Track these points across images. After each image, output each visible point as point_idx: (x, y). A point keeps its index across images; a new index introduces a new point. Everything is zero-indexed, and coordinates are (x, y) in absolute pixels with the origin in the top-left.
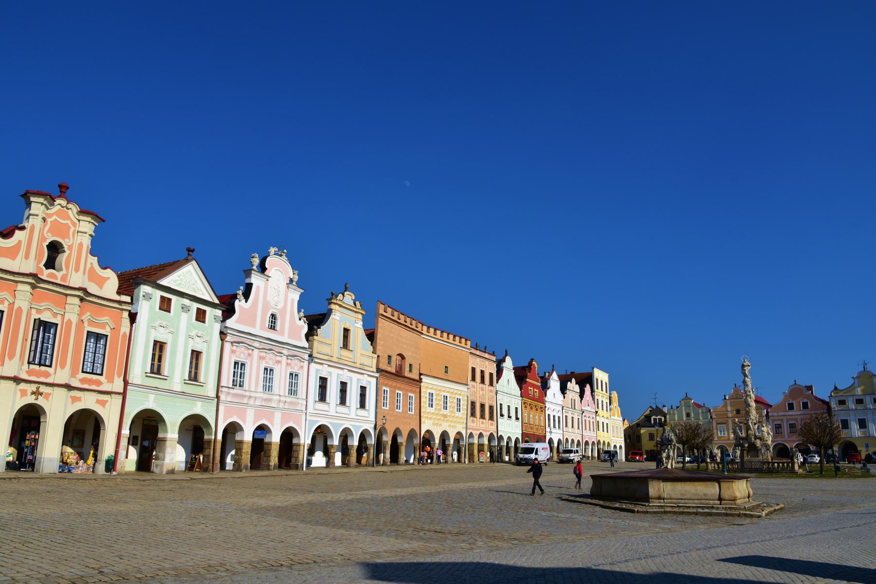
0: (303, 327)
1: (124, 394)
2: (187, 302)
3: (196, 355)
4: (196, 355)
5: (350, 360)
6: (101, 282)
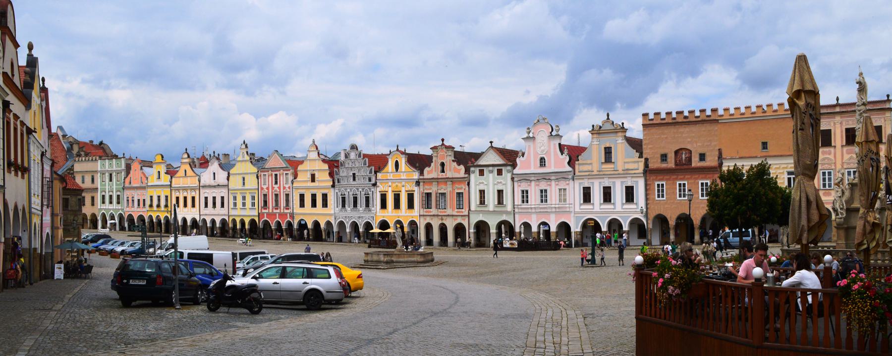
0: (565, 158)
1: (469, 216)
2: (491, 168)
3: (500, 192)
4: (500, 192)
5: (613, 169)
6: (458, 171)
